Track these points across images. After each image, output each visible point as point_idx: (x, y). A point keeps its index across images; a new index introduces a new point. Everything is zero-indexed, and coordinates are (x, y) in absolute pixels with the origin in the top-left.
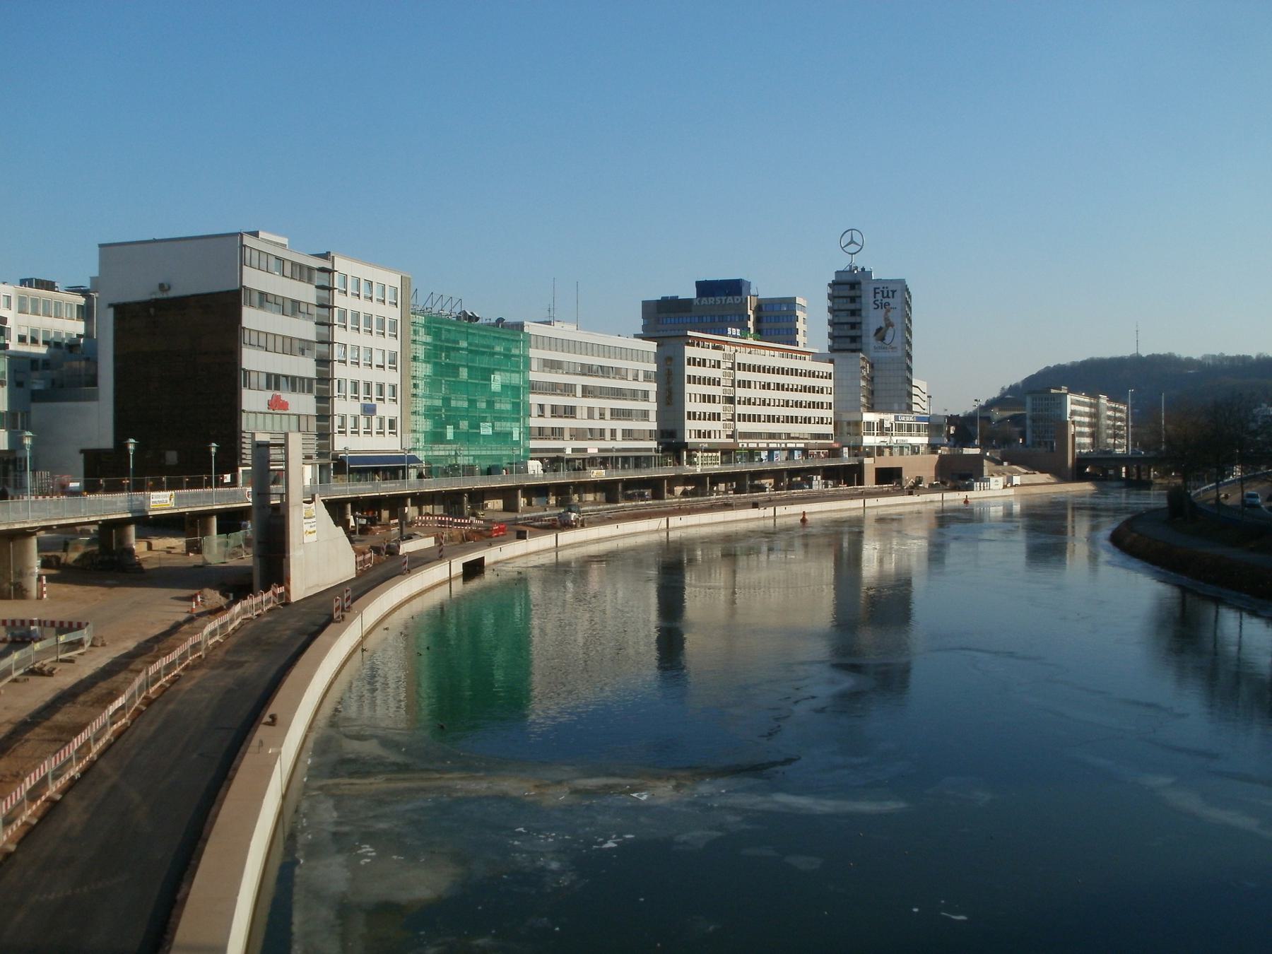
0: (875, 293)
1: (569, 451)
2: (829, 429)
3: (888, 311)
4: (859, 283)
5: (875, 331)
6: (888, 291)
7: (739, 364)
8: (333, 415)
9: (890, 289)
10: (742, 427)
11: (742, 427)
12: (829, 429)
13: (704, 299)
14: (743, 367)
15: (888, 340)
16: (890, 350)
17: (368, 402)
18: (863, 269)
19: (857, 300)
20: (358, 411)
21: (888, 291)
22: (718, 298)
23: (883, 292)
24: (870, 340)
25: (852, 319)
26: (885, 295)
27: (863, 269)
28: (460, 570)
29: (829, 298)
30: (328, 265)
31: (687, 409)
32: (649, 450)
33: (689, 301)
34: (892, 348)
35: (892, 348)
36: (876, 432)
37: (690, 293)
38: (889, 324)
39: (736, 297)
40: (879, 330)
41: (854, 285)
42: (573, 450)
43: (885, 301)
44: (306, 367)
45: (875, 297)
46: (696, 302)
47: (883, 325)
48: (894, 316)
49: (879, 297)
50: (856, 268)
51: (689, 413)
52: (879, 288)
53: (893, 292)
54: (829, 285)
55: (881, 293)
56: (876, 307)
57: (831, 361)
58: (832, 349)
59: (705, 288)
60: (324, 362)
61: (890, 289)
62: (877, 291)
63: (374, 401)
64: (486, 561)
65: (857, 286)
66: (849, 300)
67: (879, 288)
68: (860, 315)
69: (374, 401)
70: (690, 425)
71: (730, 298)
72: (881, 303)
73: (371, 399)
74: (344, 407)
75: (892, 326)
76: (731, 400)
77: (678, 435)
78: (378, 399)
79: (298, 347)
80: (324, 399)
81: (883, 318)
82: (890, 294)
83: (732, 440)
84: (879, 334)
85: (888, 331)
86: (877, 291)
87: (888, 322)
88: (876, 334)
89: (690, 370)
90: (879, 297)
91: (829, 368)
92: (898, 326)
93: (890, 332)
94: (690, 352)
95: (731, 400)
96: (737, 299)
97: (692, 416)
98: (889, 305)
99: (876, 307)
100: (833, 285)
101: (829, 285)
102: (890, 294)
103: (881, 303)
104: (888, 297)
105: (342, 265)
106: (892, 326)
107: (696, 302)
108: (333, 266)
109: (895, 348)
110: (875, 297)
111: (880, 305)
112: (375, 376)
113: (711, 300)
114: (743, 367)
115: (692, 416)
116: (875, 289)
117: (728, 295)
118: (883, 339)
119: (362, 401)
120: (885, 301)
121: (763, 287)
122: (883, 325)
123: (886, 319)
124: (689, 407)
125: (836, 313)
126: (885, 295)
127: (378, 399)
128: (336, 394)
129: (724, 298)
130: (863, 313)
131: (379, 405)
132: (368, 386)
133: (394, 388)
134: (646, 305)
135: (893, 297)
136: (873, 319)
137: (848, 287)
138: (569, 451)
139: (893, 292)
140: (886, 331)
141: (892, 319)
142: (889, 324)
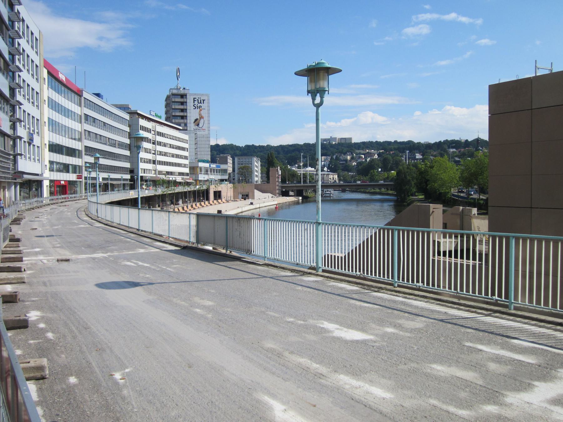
0: (194, 101)
2: (187, 170)
3: (201, 110)
4: (186, 95)
5: (194, 121)
6: (201, 100)
9: (202, 99)
10: (160, 168)
11: (160, 168)
15: (201, 125)
16: (202, 131)
19: (185, 104)
21: (201, 100)
23: (198, 100)
24: (191, 126)
25: (182, 114)
26: (199, 102)
27: (184, 89)
34: (203, 130)
35: (203, 130)
36: (203, 172)
38: (201, 117)
40: (196, 120)
41: (183, 96)
42: (104, 179)
43: (199, 105)
45: (194, 103)
47: (198, 118)
48: (204, 113)
49: (196, 103)
52: (196, 98)
53: (204, 100)
55: (197, 101)
56: (195, 108)
61: (202, 99)
62: (195, 99)
65: (184, 97)
66: (180, 103)
67: (196, 98)
70: (142, 166)
72: (197, 106)
75: (203, 118)
77: (135, 171)
81: (198, 114)
82: (202, 102)
84: (197, 122)
85: (201, 121)
86: (195, 99)
87: (200, 116)
88: (194, 122)
90: (196, 103)
92: (206, 118)
93: (202, 121)
98: (201, 107)
99: (195, 108)
102: (202, 102)
103: (197, 106)
104: (201, 103)
106: (203, 118)
109: (205, 129)
110: (194, 103)
111: (197, 107)
116: (194, 98)
118: (198, 125)
120: (199, 105)
122: (198, 118)
123: (200, 114)
126: (199, 102)
130: (188, 111)
135: (203, 103)
136: (192, 114)
137: (180, 97)
139: (204, 100)
140: (200, 120)
141: (203, 115)
142: (201, 117)
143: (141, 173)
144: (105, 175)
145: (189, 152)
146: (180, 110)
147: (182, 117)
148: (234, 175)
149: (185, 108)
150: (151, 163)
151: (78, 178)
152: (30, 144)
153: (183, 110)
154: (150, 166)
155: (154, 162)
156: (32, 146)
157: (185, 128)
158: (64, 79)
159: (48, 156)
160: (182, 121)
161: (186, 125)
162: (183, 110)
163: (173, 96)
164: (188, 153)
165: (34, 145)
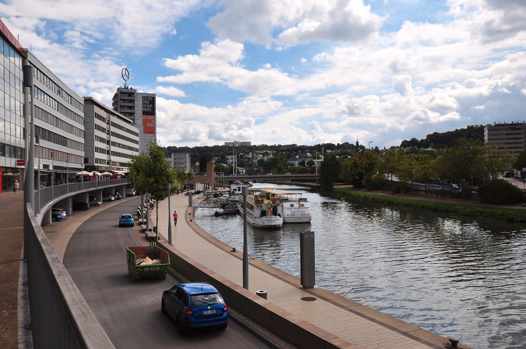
1: (51, 168)
4: (133, 94)
10: (114, 158)
18: (131, 88)
42: (55, 167)
50: (128, 88)
68: (134, 109)
83: (109, 166)
125: (122, 107)
130: (136, 108)
138: (51, 168)
143: (96, 163)
145: (140, 146)
146: (128, 108)
148: (503, 135)
149: (133, 105)
150: (105, 154)
151: (18, 165)
153: (130, 108)
154: (104, 157)
155: (108, 152)
162: (130, 108)
163: (122, 94)
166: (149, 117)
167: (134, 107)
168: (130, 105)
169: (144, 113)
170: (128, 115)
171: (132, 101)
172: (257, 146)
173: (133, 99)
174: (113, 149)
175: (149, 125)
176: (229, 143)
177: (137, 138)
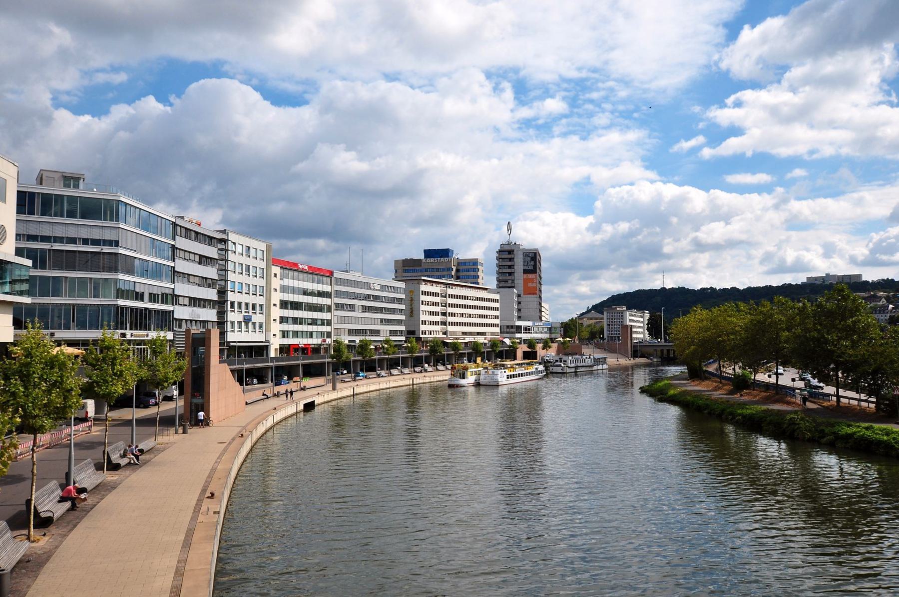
1: (358, 342)
7: (449, 295)
8: (227, 321)
10: (450, 329)
12: (497, 330)
13: (429, 259)
14: (452, 296)
17: (247, 314)
18: (515, 244)
20: (241, 319)
22: (436, 259)
25: (509, 271)
28: (302, 407)
29: (497, 259)
30: (224, 237)
31: (421, 319)
32: (401, 341)
33: (420, 260)
37: (422, 257)
39: (445, 259)
41: (510, 252)
44: (211, 294)
46: (424, 261)
51: (422, 321)
54: (497, 252)
57: (498, 293)
58: (499, 287)
59: (429, 253)
60: (222, 292)
63: (251, 314)
64: (316, 403)
68: (514, 268)
69: (251, 314)
71: (442, 259)
73: (248, 312)
74: (233, 316)
76: (444, 314)
78: (252, 313)
79: (206, 282)
80: (222, 314)
83: (445, 336)
89: (423, 298)
91: (497, 297)
94: (424, 287)
95: (444, 314)
96: (446, 259)
97: (424, 323)
100: (500, 252)
101: (497, 252)
105: (232, 237)
107: (424, 261)
108: (228, 238)
112: (251, 299)
113: (432, 260)
114: (452, 296)
115: (424, 323)
117: (441, 257)
119: (244, 313)
121: (462, 254)
124: (423, 317)
125: (501, 267)
127: (252, 313)
128: (229, 309)
129: (439, 259)
130: (515, 267)
131: (253, 316)
132: (247, 305)
133: (261, 306)
134: (396, 262)
144: (362, 338)
147: (510, 274)
152: (247, 324)
153: (510, 267)
154: (438, 328)
156: (250, 324)
157: (513, 285)
158: (306, 268)
159: (276, 327)
160: (510, 277)
161: (513, 281)
162: (510, 267)
164: (499, 312)
165: (254, 324)
166: (531, 276)
167: (514, 265)
168: (509, 263)
169: (526, 272)
170: (507, 274)
171: (511, 260)
172: (871, 281)
173: (513, 257)
174: (450, 319)
175: (530, 285)
176: (816, 279)
177: (497, 305)
